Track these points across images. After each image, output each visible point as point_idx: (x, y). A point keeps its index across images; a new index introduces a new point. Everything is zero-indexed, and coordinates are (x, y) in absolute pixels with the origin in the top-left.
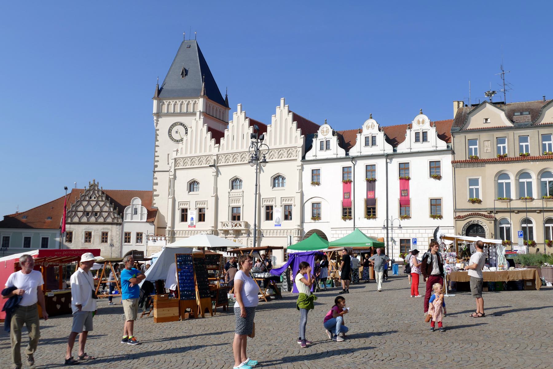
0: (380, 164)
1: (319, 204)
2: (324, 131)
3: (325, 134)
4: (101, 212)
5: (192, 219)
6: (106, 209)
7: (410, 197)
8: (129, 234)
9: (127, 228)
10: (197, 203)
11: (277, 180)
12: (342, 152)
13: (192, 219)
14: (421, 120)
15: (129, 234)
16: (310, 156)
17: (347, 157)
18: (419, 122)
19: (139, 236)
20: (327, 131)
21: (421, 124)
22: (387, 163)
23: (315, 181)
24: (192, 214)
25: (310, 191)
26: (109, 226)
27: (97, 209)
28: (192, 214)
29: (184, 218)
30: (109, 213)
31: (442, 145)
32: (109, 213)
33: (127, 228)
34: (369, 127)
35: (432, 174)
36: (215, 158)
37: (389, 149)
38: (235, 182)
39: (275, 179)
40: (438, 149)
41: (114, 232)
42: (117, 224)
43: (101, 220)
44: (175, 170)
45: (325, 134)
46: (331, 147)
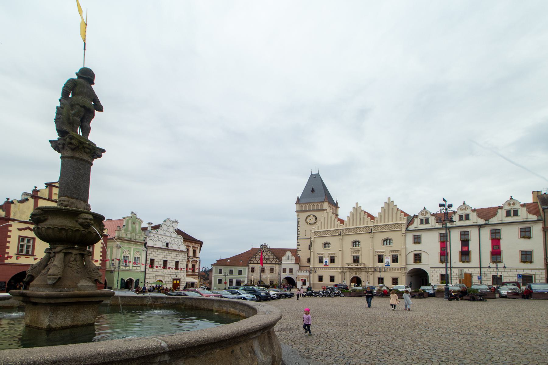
4: (269, 258)
5: (326, 262)
6: (271, 257)
7: (501, 250)
8: (285, 269)
9: (283, 266)
10: (329, 254)
11: (387, 241)
13: (326, 262)
15: (285, 269)
19: (291, 271)
23: (416, 241)
24: (326, 259)
26: (274, 265)
27: (267, 257)
28: (326, 259)
29: (321, 261)
30: (274, 258)
31: (534, 217)
32: (274, 258)
33: (283, 266)
35: (524, 235)
37: (481, 221)
38: (355, 243)
39: (384, 241)
40: (528, 220)
41: (276, 268)
42: (278, 264)
43: (269, 262)
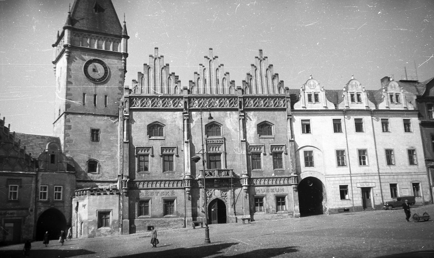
0: (367, 120)
1: (311, 152)
2: (311, 85)
3: (312, 87)
12: (331, 107)
14: (393, 85)
16: (298, 106)
17: (337, 111)
18: (392, 87)
20: (313, 85)
21: (393, 89)
22: (372, 119)
25: (302, 140)
34: (353, 86)
36: (187, 100)
44: (131, 110)
45: (312, 87)
46: (320, 100)
